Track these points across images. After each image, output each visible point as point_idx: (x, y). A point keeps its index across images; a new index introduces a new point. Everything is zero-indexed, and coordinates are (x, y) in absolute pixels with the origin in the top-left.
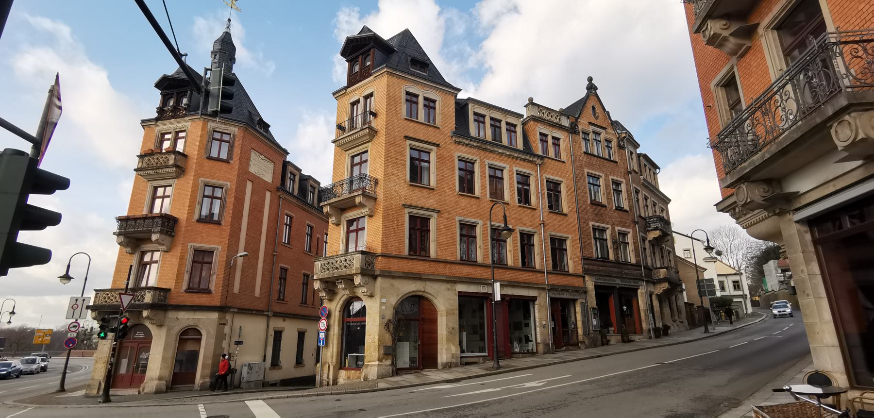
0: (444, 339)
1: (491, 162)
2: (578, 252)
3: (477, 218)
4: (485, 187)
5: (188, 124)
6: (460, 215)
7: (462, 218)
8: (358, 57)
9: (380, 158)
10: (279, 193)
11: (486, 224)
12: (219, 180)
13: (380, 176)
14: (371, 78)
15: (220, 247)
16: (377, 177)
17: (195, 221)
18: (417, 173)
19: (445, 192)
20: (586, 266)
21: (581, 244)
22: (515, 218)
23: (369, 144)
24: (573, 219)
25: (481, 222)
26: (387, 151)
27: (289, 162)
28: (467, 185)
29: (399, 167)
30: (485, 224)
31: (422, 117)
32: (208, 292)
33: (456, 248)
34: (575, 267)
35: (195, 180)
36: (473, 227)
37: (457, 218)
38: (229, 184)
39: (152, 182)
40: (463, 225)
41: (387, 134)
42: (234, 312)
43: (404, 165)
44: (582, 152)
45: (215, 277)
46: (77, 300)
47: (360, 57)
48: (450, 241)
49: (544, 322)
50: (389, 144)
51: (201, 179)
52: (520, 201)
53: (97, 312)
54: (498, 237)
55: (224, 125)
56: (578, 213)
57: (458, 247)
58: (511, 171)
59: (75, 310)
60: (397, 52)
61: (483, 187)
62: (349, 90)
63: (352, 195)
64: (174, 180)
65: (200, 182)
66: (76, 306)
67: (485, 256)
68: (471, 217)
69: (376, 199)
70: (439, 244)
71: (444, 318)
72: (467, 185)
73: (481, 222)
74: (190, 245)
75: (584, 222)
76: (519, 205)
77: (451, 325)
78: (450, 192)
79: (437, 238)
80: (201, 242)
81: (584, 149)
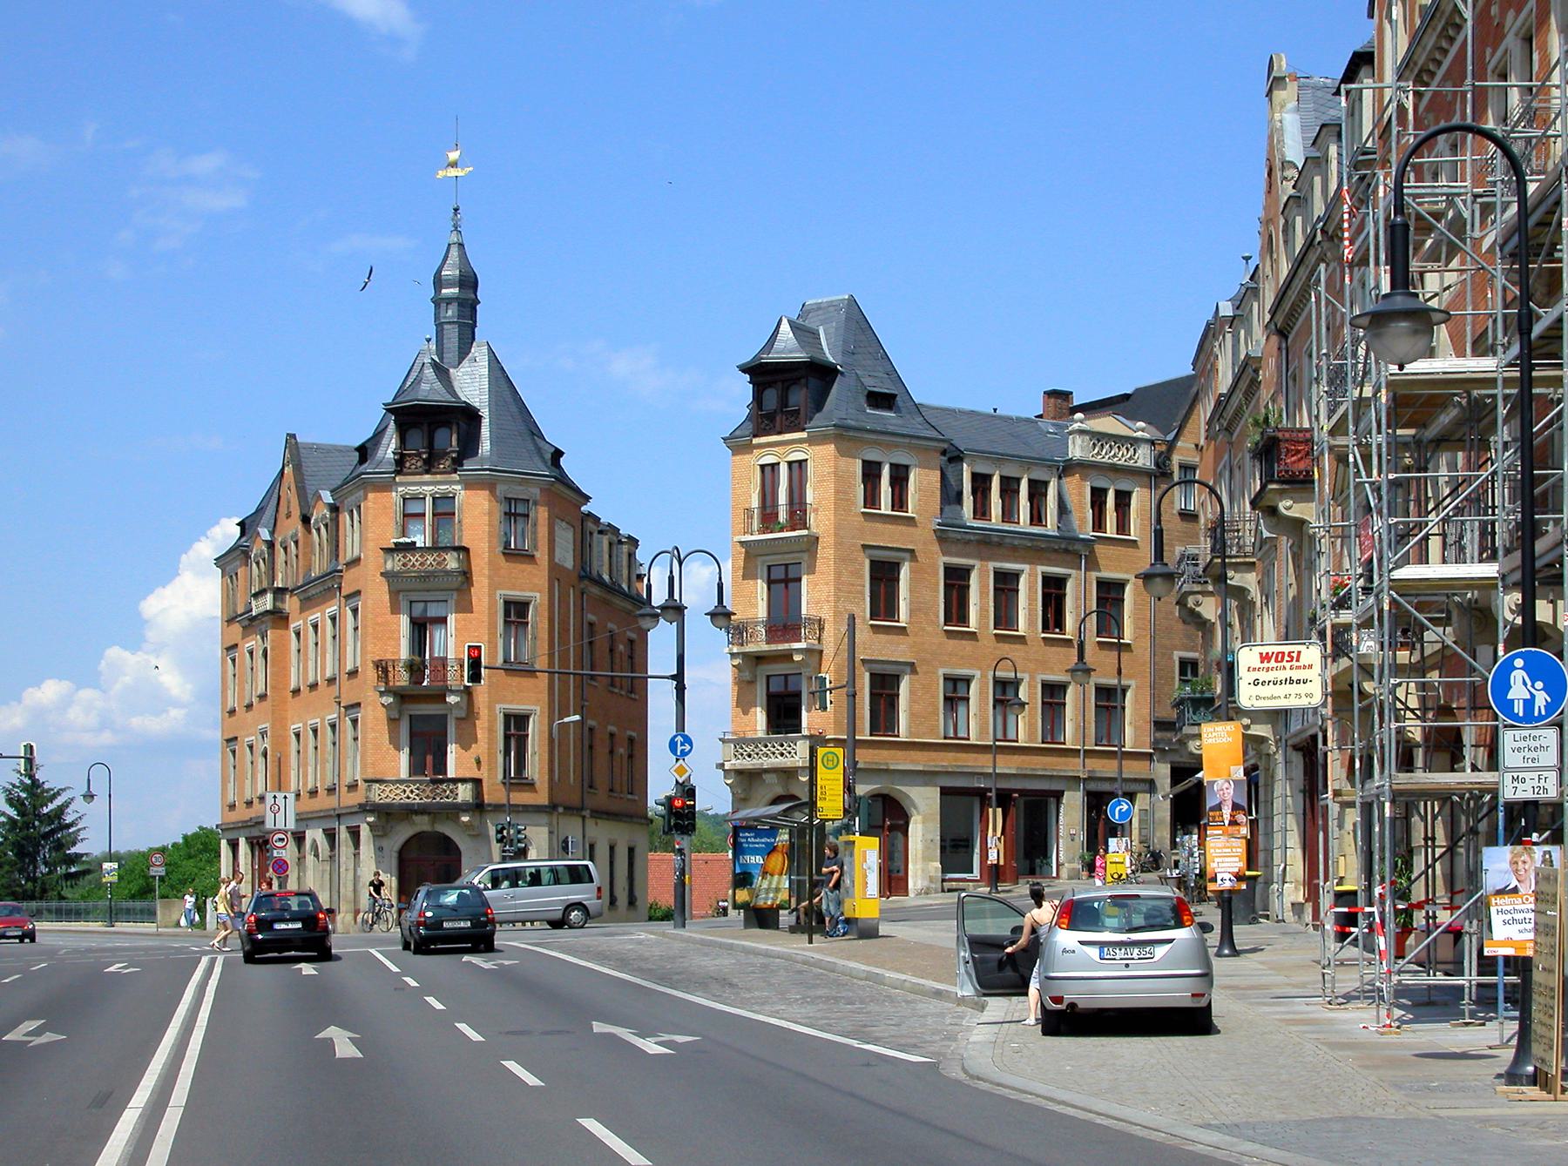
0: (919, 856)
1: (998, 565)
2: (1146, 711)
3: (972, 666)
4: (987, 611)
6: (943, 664)
7: (949, 671)
8: (775, 382)
9: (827, 584)
10: (582, 586)
11: (986, 676)
12: (524, 590)
13: (826, 613)
14: (804, 435)
15: (538, 708)
16: (823, 617)
18: (883, 602)
19: (924, 629)
20: (1158, 735)
21: (1153, 696)
22: (1036, 660)
24: (1143, 650)
25: (978, 674)
26: (838, 575)
27: (590, 514)
28: (956, 609)
29: (854, 598)
30: (984, 676)
31: (885, 507)
32: (530, 786)
33: (938, 720)
34: (1136, 737)
35: (491, 596)
36: (967, 681)
37: (941, 672)
38: (538, 595)
40: (947, 678)
41: (838, 545)
42: (560, 814)
43: (863, 593)
44: (1175, 512)
45: (537, 758)
47: (780, 384)
48: (930, 709)
49: (1073, 832)
50: (842, 560)
51: (498, 592)
52: (1045, 628)
54: (1005, 693)
56: (1153, 638)
57: (942, 716)
58: (1032, 575)
60: (842, 373)
61: (983, 611)
62: (755, 441)
64: (450, 593)
65: (498, 598)
67: (982, 731)
68: (962, 666)
69: (822, 651)
70: (912, 715)
71: (920, 826)
72: (956, 609)
73: (978, 674)
74: (498, 706)
75: (1164, 654)
76: (1043, 635)
77: (930, 837)
78: (930, 629)
79: (911, 707)
80: (511, 702)
81: (1177, 507)
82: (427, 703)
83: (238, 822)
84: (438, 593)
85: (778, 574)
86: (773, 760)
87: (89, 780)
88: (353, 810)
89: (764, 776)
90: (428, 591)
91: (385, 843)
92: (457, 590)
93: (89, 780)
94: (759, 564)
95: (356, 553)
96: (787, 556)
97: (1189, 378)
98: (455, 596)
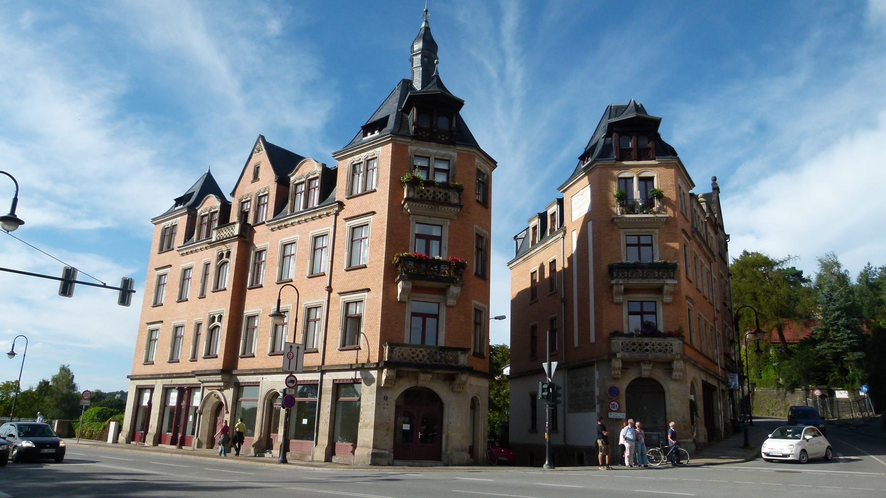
5: (455, 155)
17: (474, 275)
23: (657, 231)
39: (416, 216)
46: (291, 347)
53: (396, 370)
55: (484, 163)
59: (291, 360)
63: (661, 282)
64: (446, 220)
66: (292, 355)
82: (427, 293)
83: (251, 370)
84: (438, 219)
85: (634, 240)
86: (654, 353)
87: (13, 345)
88: (346, 368)
89: (642, 364)
90: (430, 217)
91: (389, 394)
92: (451, 219)
93: (13, 345)
94: (621, 233)
95: (373, 188)
96: (642, 230)
97: (711, 193)
98: (449, 223)
